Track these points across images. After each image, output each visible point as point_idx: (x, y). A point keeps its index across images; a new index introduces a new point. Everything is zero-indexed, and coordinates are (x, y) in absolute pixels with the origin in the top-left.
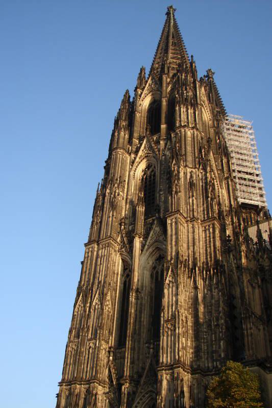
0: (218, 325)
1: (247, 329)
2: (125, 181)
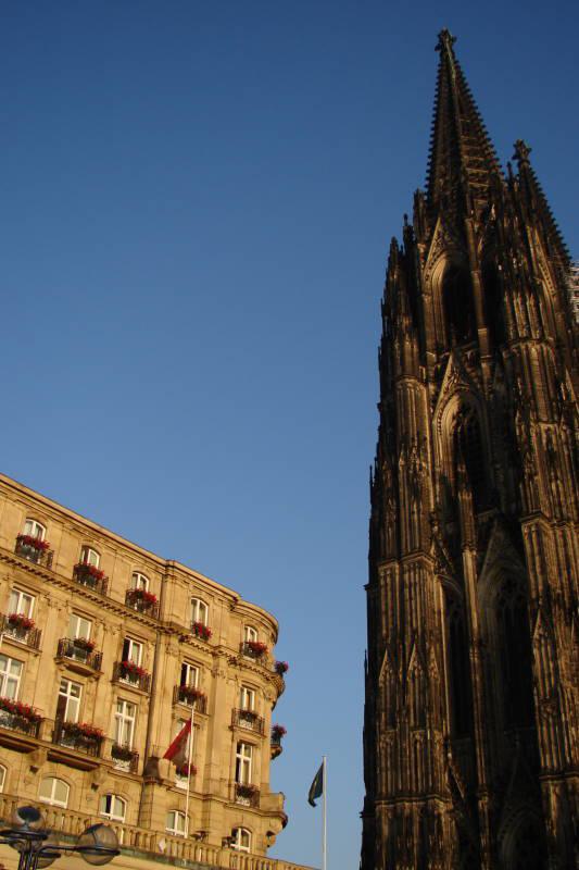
2: (425, 439)
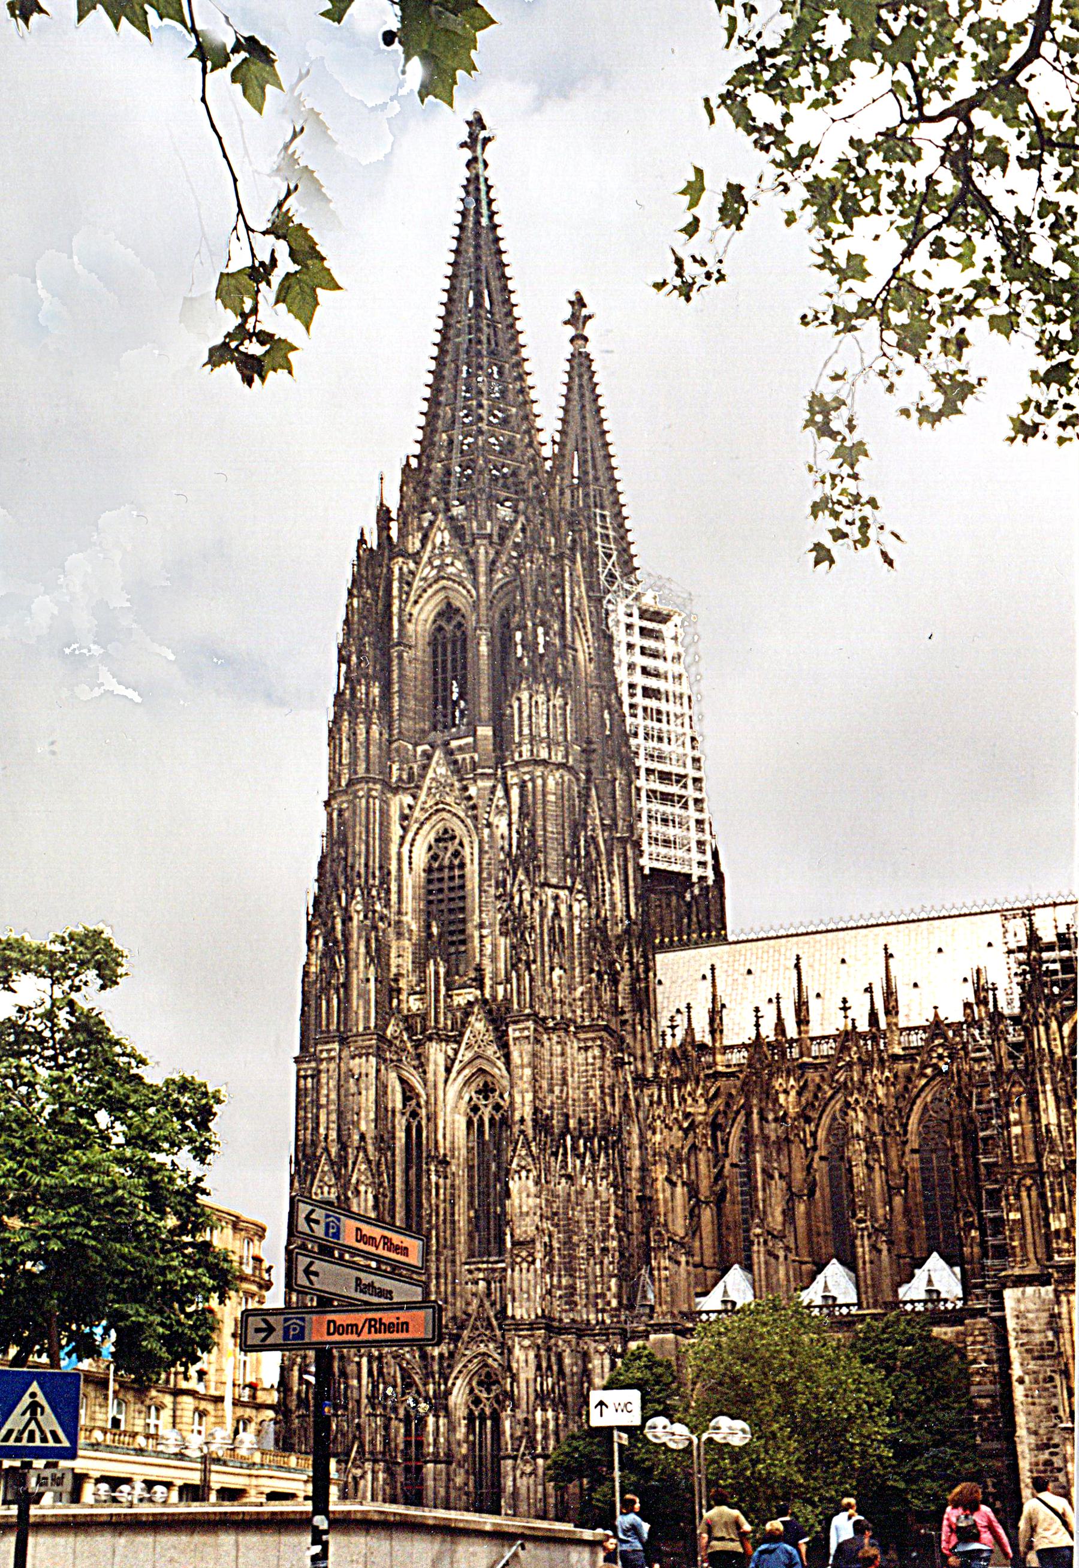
0: (605, 1250)
1: (659, 1269)
